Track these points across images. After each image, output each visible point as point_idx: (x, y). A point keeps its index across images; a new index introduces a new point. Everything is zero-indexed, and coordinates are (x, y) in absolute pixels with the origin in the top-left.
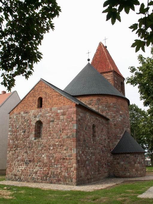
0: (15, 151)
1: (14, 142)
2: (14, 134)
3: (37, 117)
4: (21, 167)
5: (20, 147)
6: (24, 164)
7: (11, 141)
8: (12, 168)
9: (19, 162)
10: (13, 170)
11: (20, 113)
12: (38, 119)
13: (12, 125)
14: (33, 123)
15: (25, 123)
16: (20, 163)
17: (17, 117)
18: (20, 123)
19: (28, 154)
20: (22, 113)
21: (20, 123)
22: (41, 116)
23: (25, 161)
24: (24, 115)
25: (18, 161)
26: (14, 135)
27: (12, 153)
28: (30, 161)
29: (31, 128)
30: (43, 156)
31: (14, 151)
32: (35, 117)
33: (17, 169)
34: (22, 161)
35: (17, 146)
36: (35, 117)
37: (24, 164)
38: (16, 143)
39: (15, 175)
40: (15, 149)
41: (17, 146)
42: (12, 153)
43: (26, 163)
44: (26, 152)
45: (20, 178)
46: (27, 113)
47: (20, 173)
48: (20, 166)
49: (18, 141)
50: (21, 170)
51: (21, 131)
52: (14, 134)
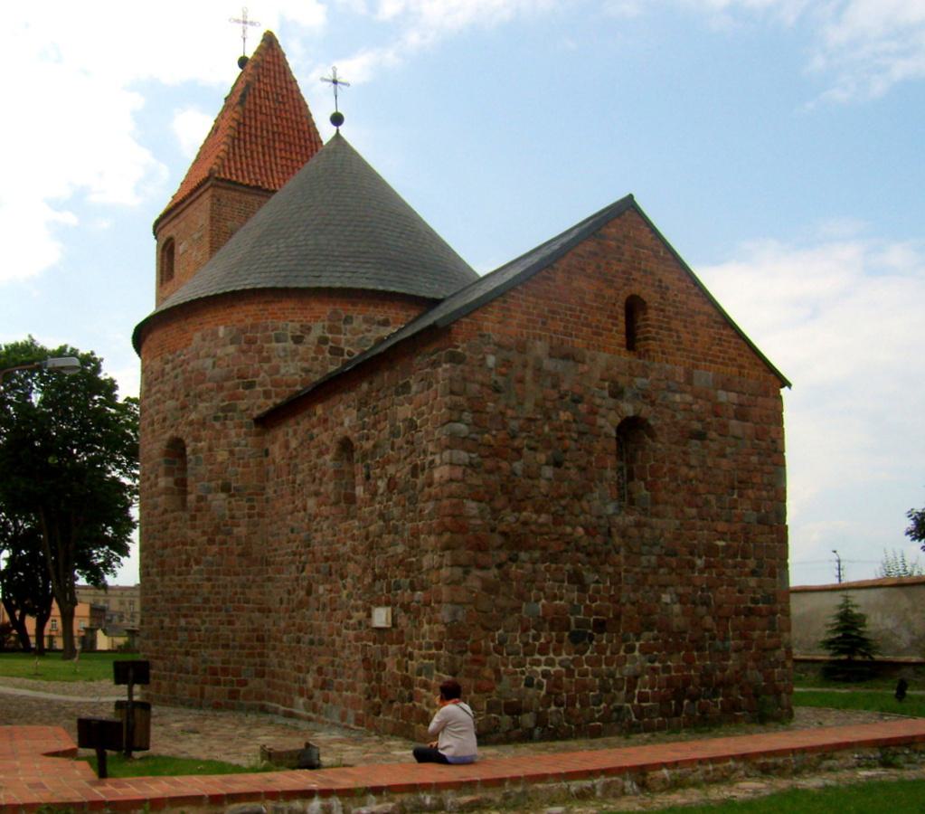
0: (499, 566)
1: (495, 511)
2: (489, 463)
3: (628, 394)
4: (543, 658)
5: (530, 548)
6: (560, 641)
7: (472, 507)
8: (488, 672)
9: (533, 632)
10: (499, 679)
11: (522, 348)
12: (628, 409)
13: (477, 408)
14: (608, 424)
15: (564, 416)
16: (536, 638)
17: (507, 363)
18: (529, 406)
19: (583, 588)
20: (540, 348)
21: (529, 406)
22: (645, 396)
23: (573, 627)
24: (548, 364)
25: (525, 630)
26: (490, 472)
27: (483, 580)
28: (600, 626)
29: (598, 446)
30: (666, 598)
31: (494, 571)
32: (617, 393)
33: (523, 673)
34: (552, 629)
35: (516, 542)
36: (617, 393)
37: (560, 641)
38: (510, 519)
39: (514, 710)
40: (503, 555)
41: (516, 542)
42: (483, 580)
44: (576, 579)
45: (541, 720)
46: (567, 357)
47: (543, 692)
48: (537, 656)
49: (518, 509)
50: (545, 674)
51: (542, 457)
52: (489, 463)
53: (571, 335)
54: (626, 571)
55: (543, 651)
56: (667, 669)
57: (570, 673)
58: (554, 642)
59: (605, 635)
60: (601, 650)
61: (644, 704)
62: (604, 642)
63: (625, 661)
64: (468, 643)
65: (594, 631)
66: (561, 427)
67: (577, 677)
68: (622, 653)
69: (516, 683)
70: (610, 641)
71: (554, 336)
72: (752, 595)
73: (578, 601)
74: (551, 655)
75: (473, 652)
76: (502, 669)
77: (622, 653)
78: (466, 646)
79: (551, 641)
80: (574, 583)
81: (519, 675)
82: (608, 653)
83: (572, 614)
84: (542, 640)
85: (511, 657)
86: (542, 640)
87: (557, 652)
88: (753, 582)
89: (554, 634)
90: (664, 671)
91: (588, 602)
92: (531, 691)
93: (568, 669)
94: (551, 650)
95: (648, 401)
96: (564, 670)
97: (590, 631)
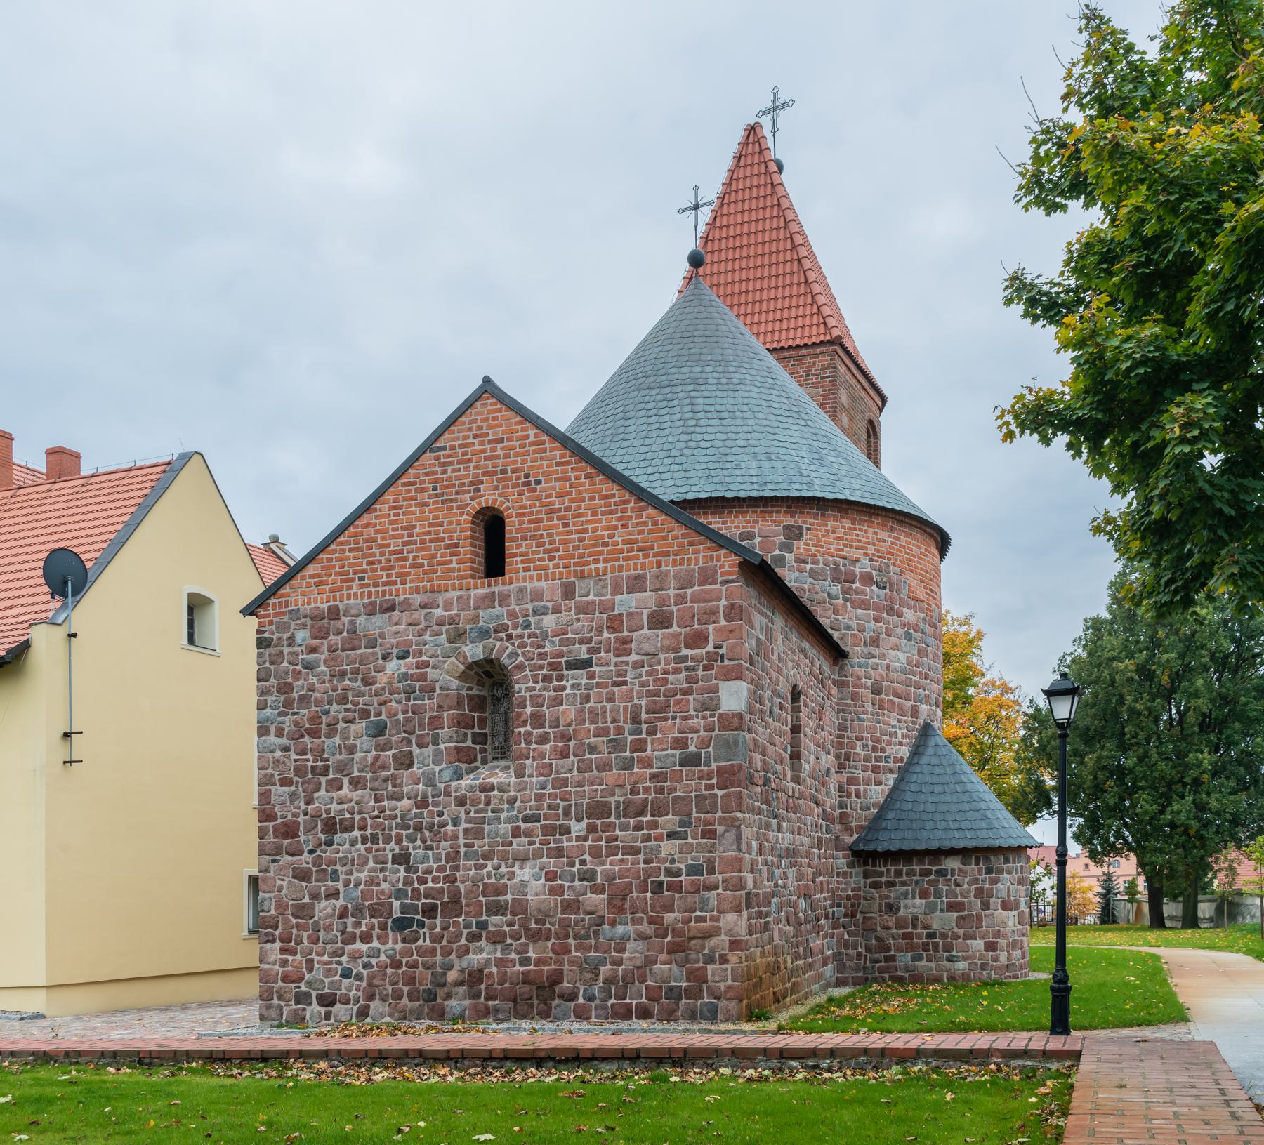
10: (310, 970)
37: (383, 927)
43: (401, 925)
44: (402, 859)
53: (395, 583)
54: (466, 845)
55: (366, 938)
56: (525, 961)
57: (396, 964)
58: (377, 930)
59: (438, 921)
60: (437, 939)
61: (490, 1003)
62: (438, 929)
63: (467, 952)
64: (277, 933)
65: (423, 917)
66: (383, 689)
67: (404, 968)
68: (463, 942)
69: (329, 973)
70: (445, 928)
71: (373, 590)
72: (668, 865)
73: (404, 884)
74: (375, 944)
75: (282, 941)
76: (316, 958)
77: (463, 942)
78: (273, 935)
79: (373, 928)
80: (400, 864)
81: (335, 966)
82: (444, 943)
83: (396, 899)
84: (364, 928)
85: (328, 946)
86: (364, 928)
87: (383, 939)
88: (667, 847)
89: (375, 921)
90: (521, 964)
91: (416, 885)
92: (346, 982)
93: (392, 958)
94: (375, 938)
95: (503, 635)
96: (388, 961)
97: (418, 917)
